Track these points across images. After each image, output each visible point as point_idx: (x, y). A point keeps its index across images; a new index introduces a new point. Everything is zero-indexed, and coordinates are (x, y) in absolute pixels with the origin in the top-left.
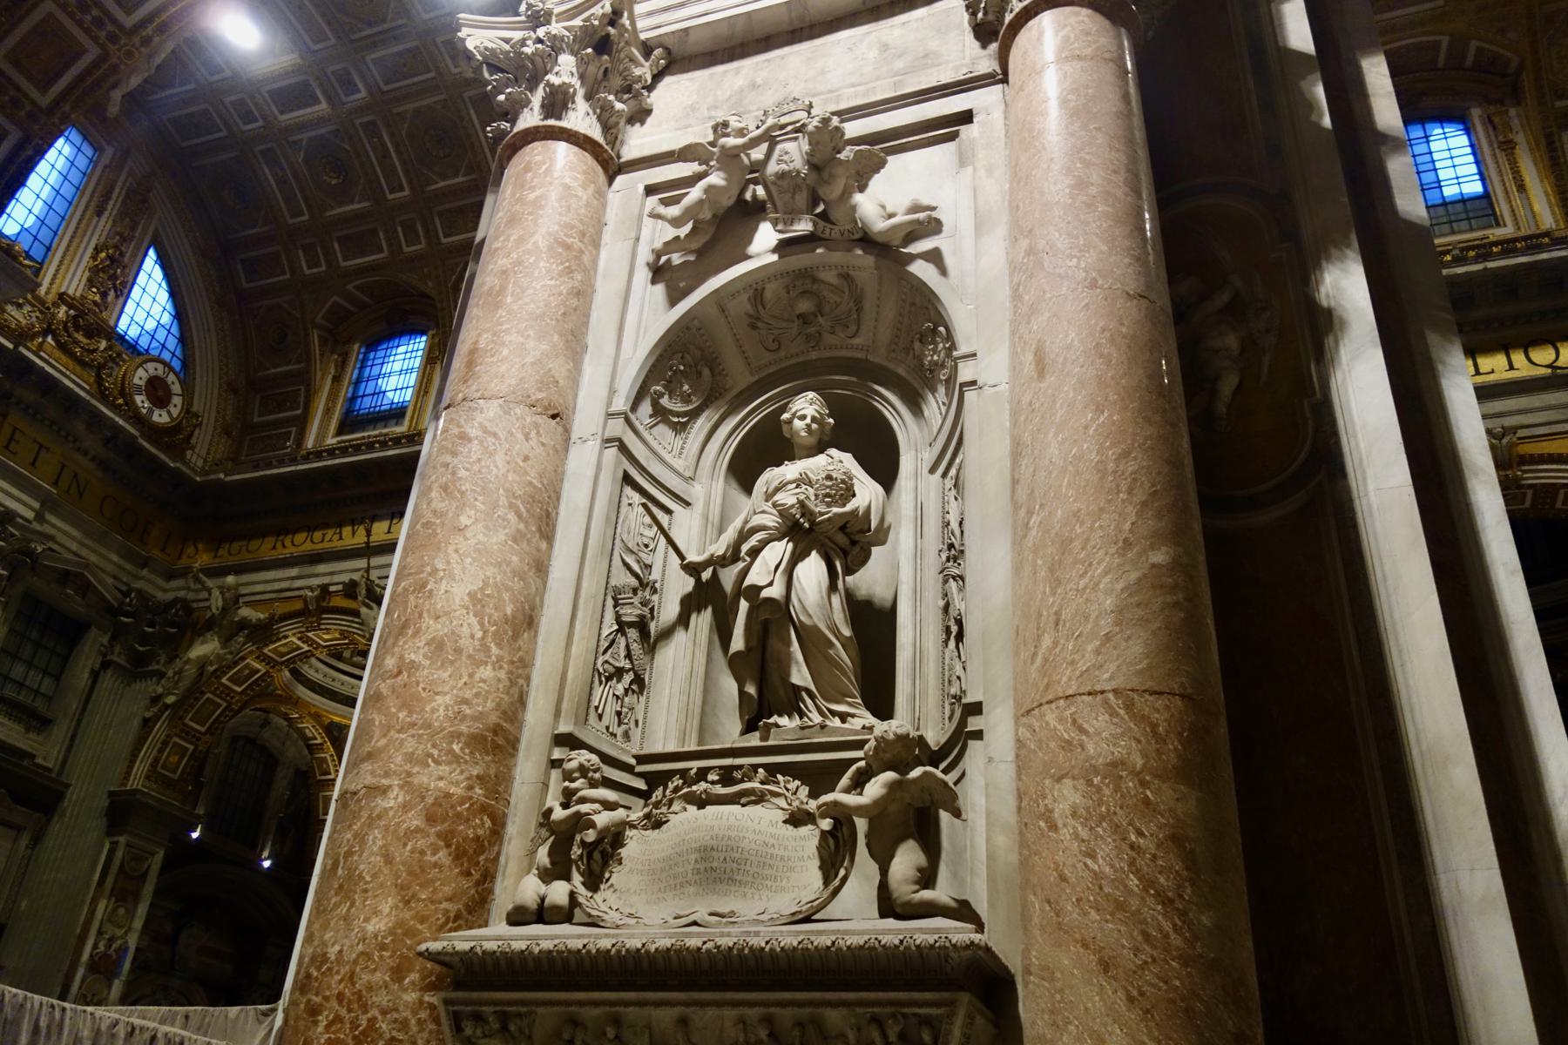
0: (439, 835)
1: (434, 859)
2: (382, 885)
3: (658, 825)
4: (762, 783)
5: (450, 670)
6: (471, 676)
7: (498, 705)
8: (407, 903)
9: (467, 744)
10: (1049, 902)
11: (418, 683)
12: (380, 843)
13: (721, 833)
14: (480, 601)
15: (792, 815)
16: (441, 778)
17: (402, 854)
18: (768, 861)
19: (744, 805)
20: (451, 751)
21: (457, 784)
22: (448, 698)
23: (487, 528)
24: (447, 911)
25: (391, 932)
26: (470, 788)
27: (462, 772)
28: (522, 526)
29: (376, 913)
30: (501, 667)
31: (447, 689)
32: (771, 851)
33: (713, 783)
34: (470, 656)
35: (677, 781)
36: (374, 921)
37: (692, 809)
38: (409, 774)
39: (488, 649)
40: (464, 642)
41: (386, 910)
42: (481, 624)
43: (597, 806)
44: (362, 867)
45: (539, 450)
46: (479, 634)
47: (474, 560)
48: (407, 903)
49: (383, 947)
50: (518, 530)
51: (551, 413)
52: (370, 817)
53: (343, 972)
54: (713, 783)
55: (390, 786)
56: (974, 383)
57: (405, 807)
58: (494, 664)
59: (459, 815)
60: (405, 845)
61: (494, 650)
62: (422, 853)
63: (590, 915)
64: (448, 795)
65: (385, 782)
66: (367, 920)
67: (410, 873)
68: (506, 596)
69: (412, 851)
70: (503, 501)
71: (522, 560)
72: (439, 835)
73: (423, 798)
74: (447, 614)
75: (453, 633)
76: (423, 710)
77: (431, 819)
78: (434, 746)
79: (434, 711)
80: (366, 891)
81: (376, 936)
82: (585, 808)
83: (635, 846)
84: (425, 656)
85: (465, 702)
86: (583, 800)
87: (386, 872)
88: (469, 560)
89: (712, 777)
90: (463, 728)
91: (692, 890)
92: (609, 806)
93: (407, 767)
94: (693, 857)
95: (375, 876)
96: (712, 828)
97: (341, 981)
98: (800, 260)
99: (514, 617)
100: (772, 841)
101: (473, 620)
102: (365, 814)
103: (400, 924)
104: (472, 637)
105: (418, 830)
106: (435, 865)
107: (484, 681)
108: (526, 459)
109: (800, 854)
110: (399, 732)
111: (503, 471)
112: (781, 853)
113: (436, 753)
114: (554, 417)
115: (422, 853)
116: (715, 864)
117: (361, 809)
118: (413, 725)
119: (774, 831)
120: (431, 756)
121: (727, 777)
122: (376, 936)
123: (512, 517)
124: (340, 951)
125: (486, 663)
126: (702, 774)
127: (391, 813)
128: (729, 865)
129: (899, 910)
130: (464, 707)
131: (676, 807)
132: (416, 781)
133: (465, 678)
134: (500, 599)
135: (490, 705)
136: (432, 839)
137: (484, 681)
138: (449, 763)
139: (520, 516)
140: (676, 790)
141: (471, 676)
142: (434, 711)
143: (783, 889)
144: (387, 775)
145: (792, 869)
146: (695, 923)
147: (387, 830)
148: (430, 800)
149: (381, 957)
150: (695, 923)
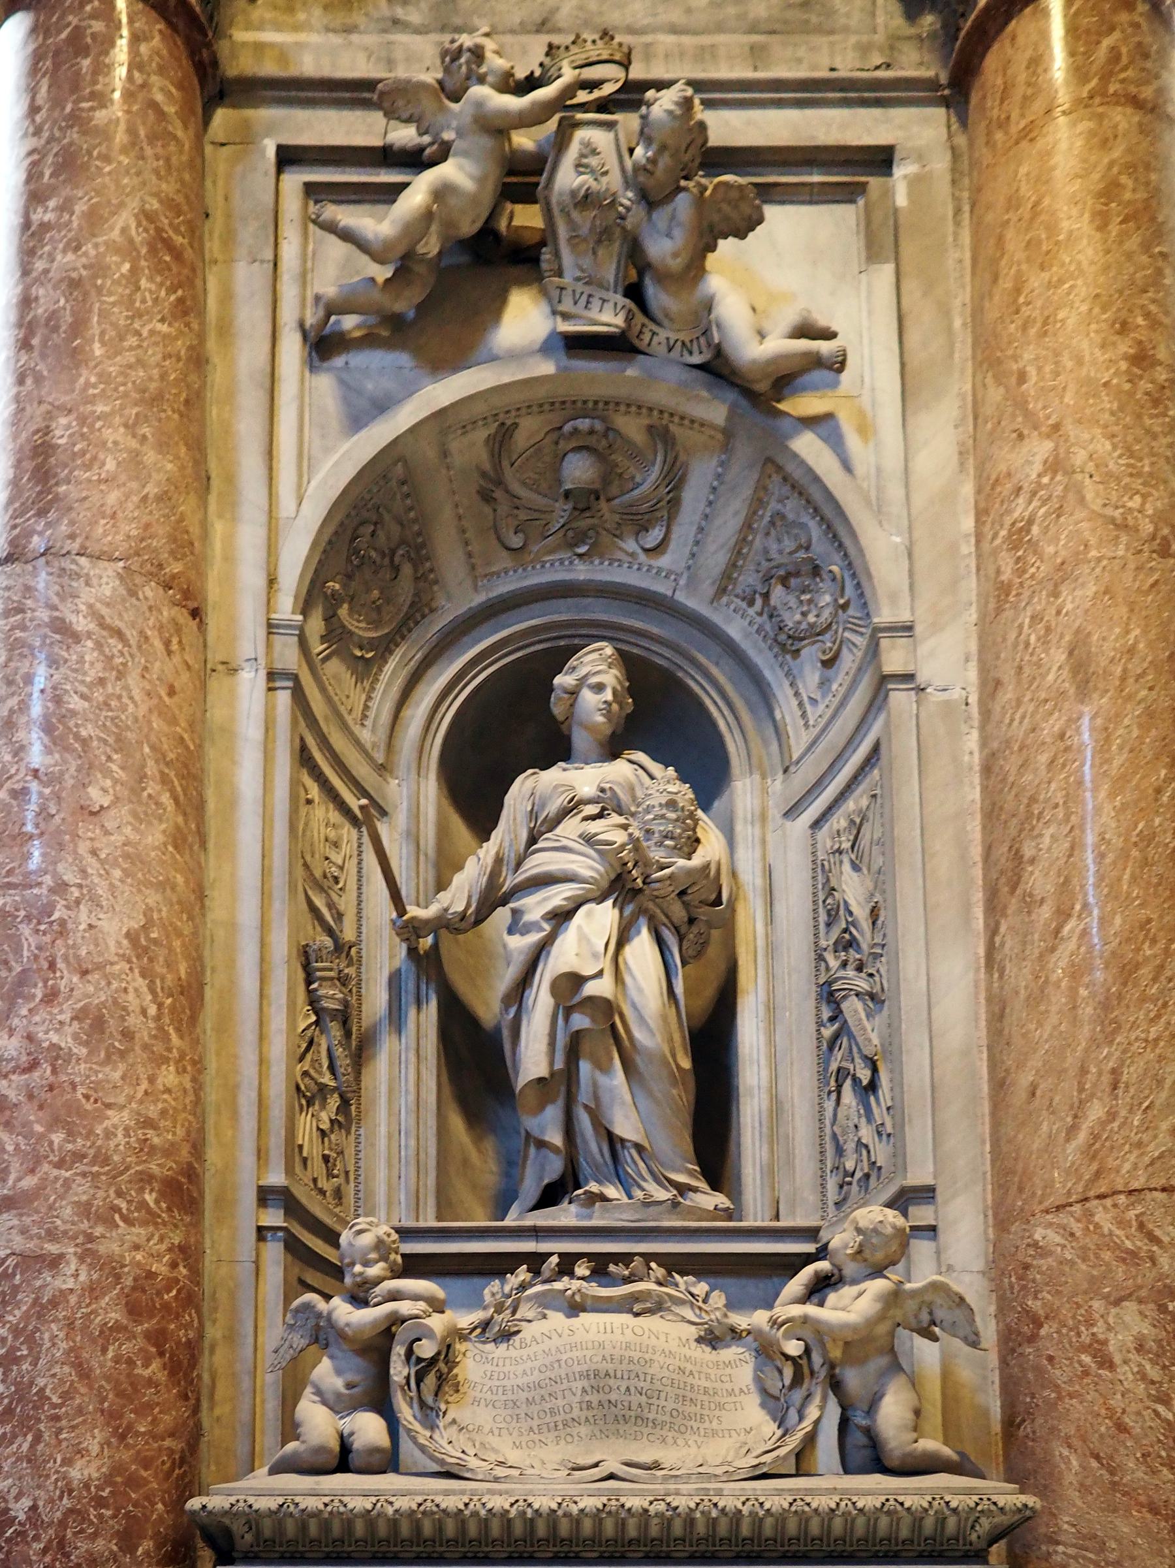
0: (148, 1335)
1: (147, 1373)
2: (80, 1411)
3: (506, 1336)
4: (660, 1284)
5: (122, 1067)
6: (152, 1080)
7: (188, 1133)
8: (122, 1437)
9: (162, 1195)
10: (1097, 1457)
11: (74, 1086)
12: (64, 1345)
13: (617, 1353)
14: (146, 950)
15: (710, 1331)
16: (137, 1247)
17: (101, 1363)
18: (689, 1395)
19: (637, 1315)
20: (143, 1204)
21: (158, 1256)
22: (125, 1114)
23: (135, 814)
24: (171, 1451)
25: (108, 1480)
26: (174, 1265)
27: (161, 1240)
28: (180, 819)
29: (81, 1452)
30: (185, 1071)
31: (121, 1100)
32: (690, 1380)
33: (583, 1278)
34: (145, 1047)
35: (523, 1274)
36: (79, 1464)
37: (557, 1319)
38: (90, 1238)
39: (166, 1038)
40: (134, 1021)
41: (95, 1449)
42: (153, 991)
43: (422, 1305)
44: (41, 1382)
45: (185, 676)
46: (152, 1010)
47: (127, 873)
48: (122, 1437)
49: (100, 1502)
50: (177, 828)
51: (192, 605)
52: (36, 1301)
53: (45, 1537)
54: (583, 1278)
55: (61, 1256)
56: (909, 677)
57: (93, 1291)
58: (177, 1062)
59: (166, 1306)
60: (104, 1350)
61: (175, 1039)
62: (130, 1362)
63: (442, 1462)
64: (151, 1275)
65: (52, 1248)
66: (68, 1462)
67: (120, 1394)
68: (177, 944)
69: (117, 1360)
70: (151, 768)
71: (187, 882)
72: (148, 1335)
73: (118, 1277)
74: (99, 967)
75: (115, 1002)
76: (91, 1132)
77: (134, 1311)
78: (119, 1194)
79: (109, 1134)
80: (57, 1418)
81: (87, 1486)
82: (405, 1307)
83: (475, 1365)
84: (76, 1036)
85: (148, 1123)
86: (394, 1296)
87: (83, 1390)
88: (117, 873)
89: (582, 1270)
90: (154, 1168)
91: (584, 1430)
92: (438, 1307)
93: (85, 1225)
94: (578, 1385)
95: (66, 1396)
96: (601, 1345)
97: (45, 1551)
98: (597, 374)
99: (190, 985)
100: (689, 1367)
101: (141, 983)
102: (26, 1299)
103: (117, 1469)
104: (144, 1012)
105: (118, 1328)
106: (150, 1382)
107: (168, 1091)
108: (172, 692)
109: (728, 1386)
110: (59, 1165)
111: (143, 710)
112: (704, 1383)
113: (124, 1205)
114: (195, 613)
115: (130, 1362)
116: (613, 1397)
117: (15, 1289)
118: (79, 1156)
119: (686, 1351)
120: (116, 1209)
121: (601, 1266)
122: (87, 1486)
123: (166, 799)
124: (34, 1508)
125: (166, 1060)
126: (567, 1264)
127: (73, 1299)
128: (635, 1399)
129: (887, 1463)
130: (150, 1133)
131: (524, 1311)
132: (102, 1249)
133: (145, 1085)
134: (171, 949)
135: (180, 1132)
136: (140, 1342)
137: (168, 1091)
138: (144, 1223)
139: (176, 800)
140: (523, 1287)
141: (152, 1080)
142: (109, 1134)
143: (714, 1433)
144: (52, 1235)
145: (720, 1406)
146: (611, 1477)
147: (71, 1325)
148: (129, 1282)
149: (100, 1517)
150: (611, 1477)
